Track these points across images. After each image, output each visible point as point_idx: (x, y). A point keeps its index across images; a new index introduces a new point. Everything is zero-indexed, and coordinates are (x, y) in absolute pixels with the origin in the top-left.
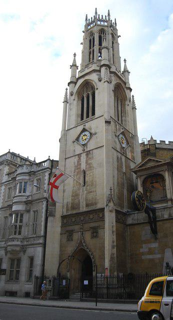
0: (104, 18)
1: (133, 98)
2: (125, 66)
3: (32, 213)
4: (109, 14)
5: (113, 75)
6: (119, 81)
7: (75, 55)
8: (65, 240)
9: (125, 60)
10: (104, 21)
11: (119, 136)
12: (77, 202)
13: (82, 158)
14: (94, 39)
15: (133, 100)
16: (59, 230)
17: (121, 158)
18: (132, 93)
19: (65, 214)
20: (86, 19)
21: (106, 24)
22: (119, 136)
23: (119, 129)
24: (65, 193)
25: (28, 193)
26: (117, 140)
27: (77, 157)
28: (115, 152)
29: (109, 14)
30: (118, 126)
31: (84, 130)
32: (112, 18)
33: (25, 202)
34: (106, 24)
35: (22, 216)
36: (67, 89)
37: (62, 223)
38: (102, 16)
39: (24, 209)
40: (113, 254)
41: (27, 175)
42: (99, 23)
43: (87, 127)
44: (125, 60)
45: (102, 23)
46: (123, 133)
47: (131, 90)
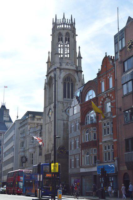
1: (83, 77)
4: (64, 17)
5: (63, 71)
7: (49, 53)
9: (79, 48)
10: (61, 24)
11: (66, 110)
15: (83, 78)
18: (83, 73)
20: (53, 23)
22: (66, 110)
26: (64, 114)
28: (62, 122)
29: (64, 17)
30: (65, 105)
32: (68, 17)
35: (33, 154)
36: (45, 80)
37: (45, 158)
38: (60, 20)
44: (79, 48)
47: (82, 71)
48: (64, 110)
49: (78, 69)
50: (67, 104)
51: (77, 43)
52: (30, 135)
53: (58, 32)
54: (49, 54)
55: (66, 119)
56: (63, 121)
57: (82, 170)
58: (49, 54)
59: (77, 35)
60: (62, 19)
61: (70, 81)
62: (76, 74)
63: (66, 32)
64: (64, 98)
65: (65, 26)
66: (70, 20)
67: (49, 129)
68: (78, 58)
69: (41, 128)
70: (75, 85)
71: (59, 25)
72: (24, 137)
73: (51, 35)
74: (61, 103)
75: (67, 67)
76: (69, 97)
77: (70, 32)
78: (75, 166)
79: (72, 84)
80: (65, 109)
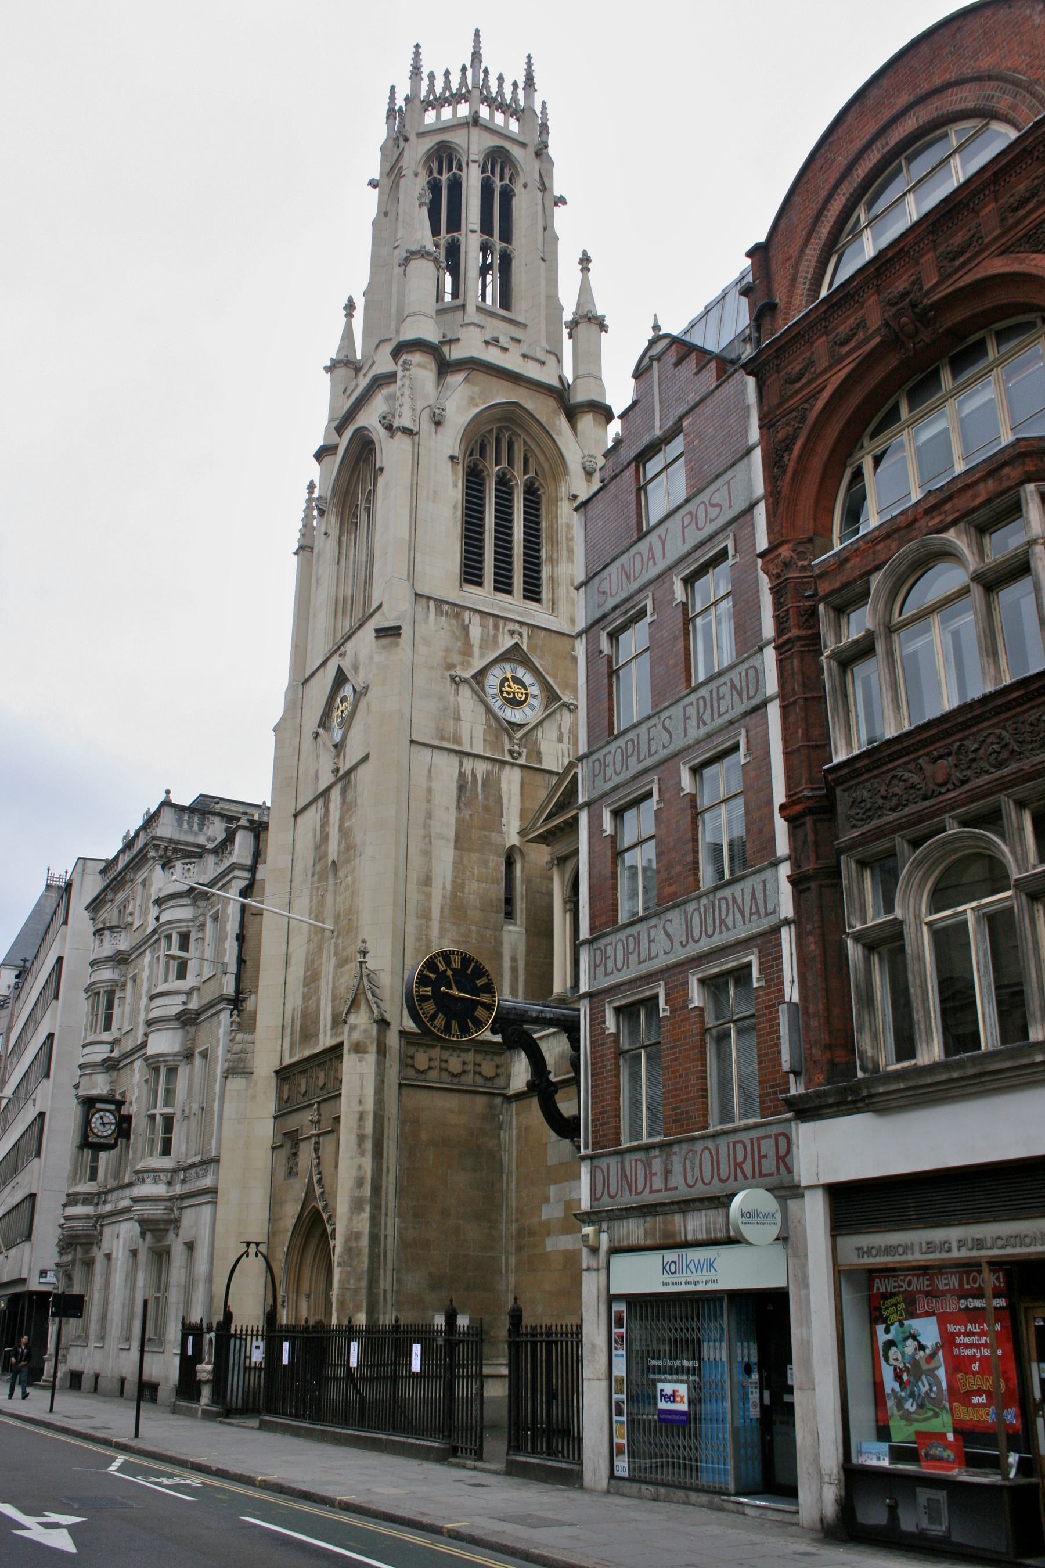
0: (455, 86)
2: (585, 289)
3: (198, 1060)
4: (476, 56)
5: (460, 377)
6: (502, 394)
7: (350, 307)
8: (281, 1172)
9: (585, 261)
10: (455, 99)
11: (482, 673)
12: (314, 1005)
13: (332, 806)
14: (456, 186)
16: (265, 1129)
17: (491, 784)
19: (287, 1061)
20: (391, 112)
21: (463, 110)
23: (488, 641)
24: (291, 970)
25: (191, 981)
26: (466, 698)
28: (447, 768)
29: (476, 56)
30: (475, 632)
31: (341, 679)
33: (178, 1017)
34: (463, 110)
36: (311, 487)
37: (279, 1099)
38: (447, 74)
39: (176, 1048)
40: (357, 1236)
41: (186, 901)
42: (430, 117)
43: (347, 665)
44: (585, 261)
45: (447, 113)
46: (515, 655)
48: (468, 674)
49: (580, 396)
50: (492, 632)
51: (560, 244)
53: (428, 144)
54: (349, 315)
56: (455, 760)
58: (349, 315)
59: (561, 201)
60: (464, 69)
61: (519, 464)
62: (563, 422)
63: (493, 144)
64: (467, 581)
65: (484, 112)
66: (515, 85)
67: (325, 838)
68: (573, 325)
69: (258, 855)
70: (557, 500)
71: (436, 103)
72: (121, 959)
73: (374, 184)
74: (439, 612)
75: (493, 356)
76: (503, 585)
77: (516, 151)
79: (532, 492)
80: (478, 664)
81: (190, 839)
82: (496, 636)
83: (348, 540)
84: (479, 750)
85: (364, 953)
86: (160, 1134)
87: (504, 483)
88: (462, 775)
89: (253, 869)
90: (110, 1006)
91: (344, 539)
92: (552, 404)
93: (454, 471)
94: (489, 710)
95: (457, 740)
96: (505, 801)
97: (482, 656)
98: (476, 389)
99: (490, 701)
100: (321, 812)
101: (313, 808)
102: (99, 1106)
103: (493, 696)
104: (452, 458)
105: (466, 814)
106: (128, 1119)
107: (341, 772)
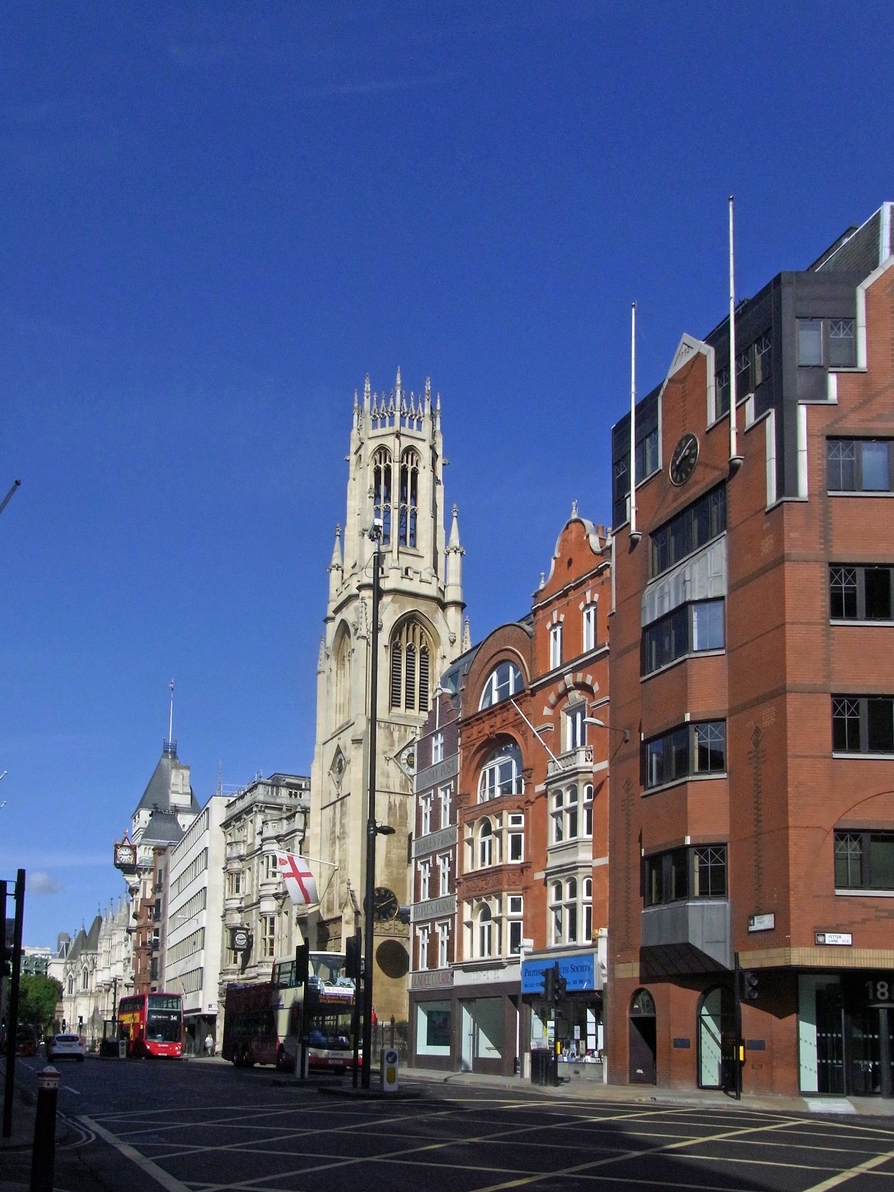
13: (337, 810)
17: (403, 805)
23: (401, 739)
27: (332, 806)
30: (396, 735)
37: (319, 935)
39: (274, 909)
48: (392, 756)
52: (265, 848)
55: (398, 790)
56: (387, 795)
57: (461, 979)
67: (334, 825)
75: (406, 585)
78: (432, 961)
79: (424, 652)
80: (397, 749)
81: (272, 800)
82: (405, 735)
83: (341, 674)
84: (397, 790)
85: (349, 884)
86: (268, 946)
87: (410, 649)
88: (390, 802)
89: (304, 831)
90: (238, 881)
91: (339, 672)
92: (434, 605)
93: (386, 652)
94: (402, 771)
95: (388, 787)
96: (409, 812)
97: (399, 745)
98: (397, 605)
99: (402, 767)
100: (332, 813)
101: (329, 807)
102: (238, 931)
103: (404, 764)
104: (385, 646)
105: (392, 819)
106: (252, 936)
107: (340, 797)
